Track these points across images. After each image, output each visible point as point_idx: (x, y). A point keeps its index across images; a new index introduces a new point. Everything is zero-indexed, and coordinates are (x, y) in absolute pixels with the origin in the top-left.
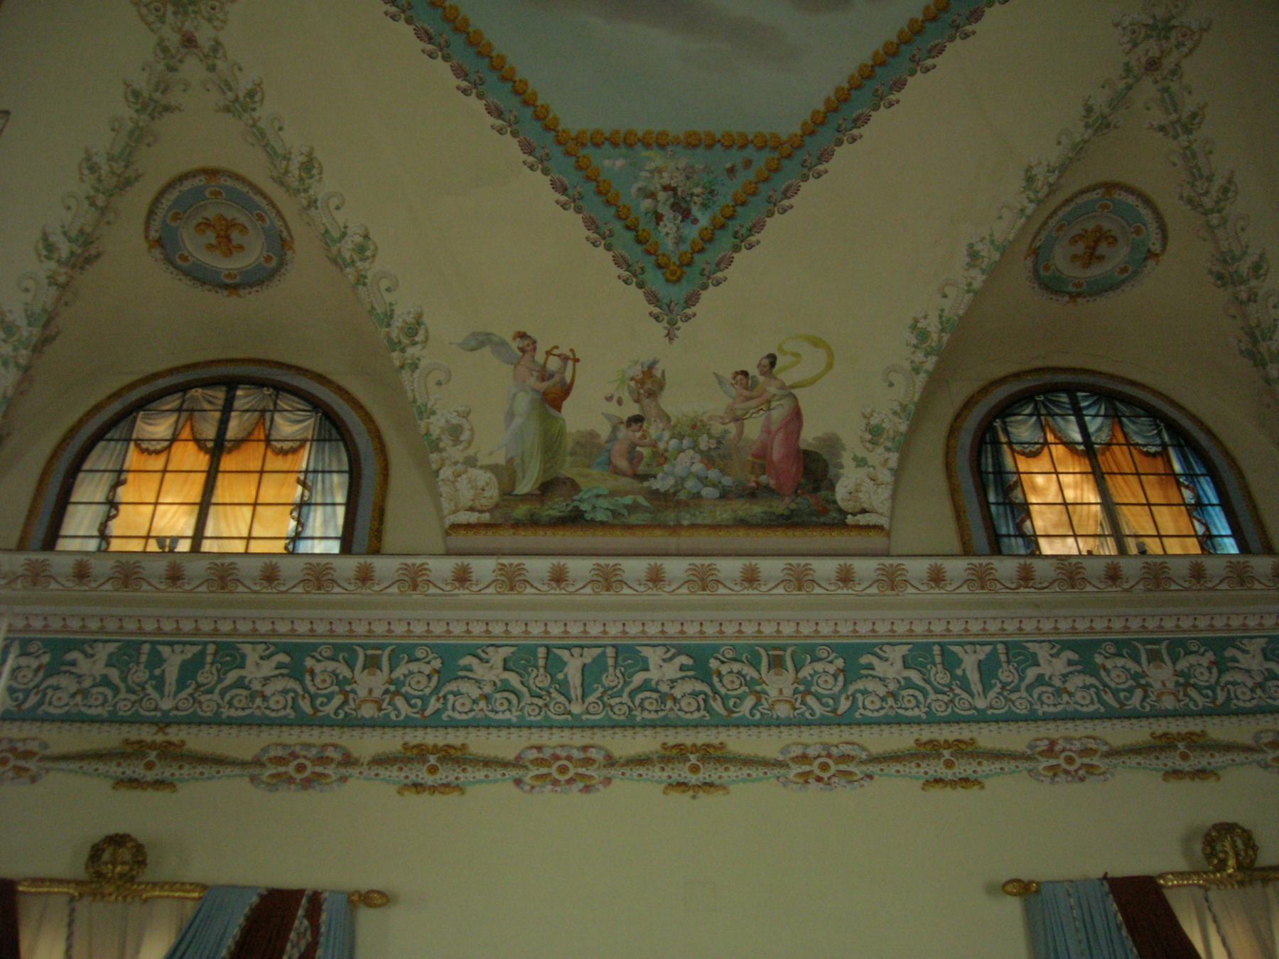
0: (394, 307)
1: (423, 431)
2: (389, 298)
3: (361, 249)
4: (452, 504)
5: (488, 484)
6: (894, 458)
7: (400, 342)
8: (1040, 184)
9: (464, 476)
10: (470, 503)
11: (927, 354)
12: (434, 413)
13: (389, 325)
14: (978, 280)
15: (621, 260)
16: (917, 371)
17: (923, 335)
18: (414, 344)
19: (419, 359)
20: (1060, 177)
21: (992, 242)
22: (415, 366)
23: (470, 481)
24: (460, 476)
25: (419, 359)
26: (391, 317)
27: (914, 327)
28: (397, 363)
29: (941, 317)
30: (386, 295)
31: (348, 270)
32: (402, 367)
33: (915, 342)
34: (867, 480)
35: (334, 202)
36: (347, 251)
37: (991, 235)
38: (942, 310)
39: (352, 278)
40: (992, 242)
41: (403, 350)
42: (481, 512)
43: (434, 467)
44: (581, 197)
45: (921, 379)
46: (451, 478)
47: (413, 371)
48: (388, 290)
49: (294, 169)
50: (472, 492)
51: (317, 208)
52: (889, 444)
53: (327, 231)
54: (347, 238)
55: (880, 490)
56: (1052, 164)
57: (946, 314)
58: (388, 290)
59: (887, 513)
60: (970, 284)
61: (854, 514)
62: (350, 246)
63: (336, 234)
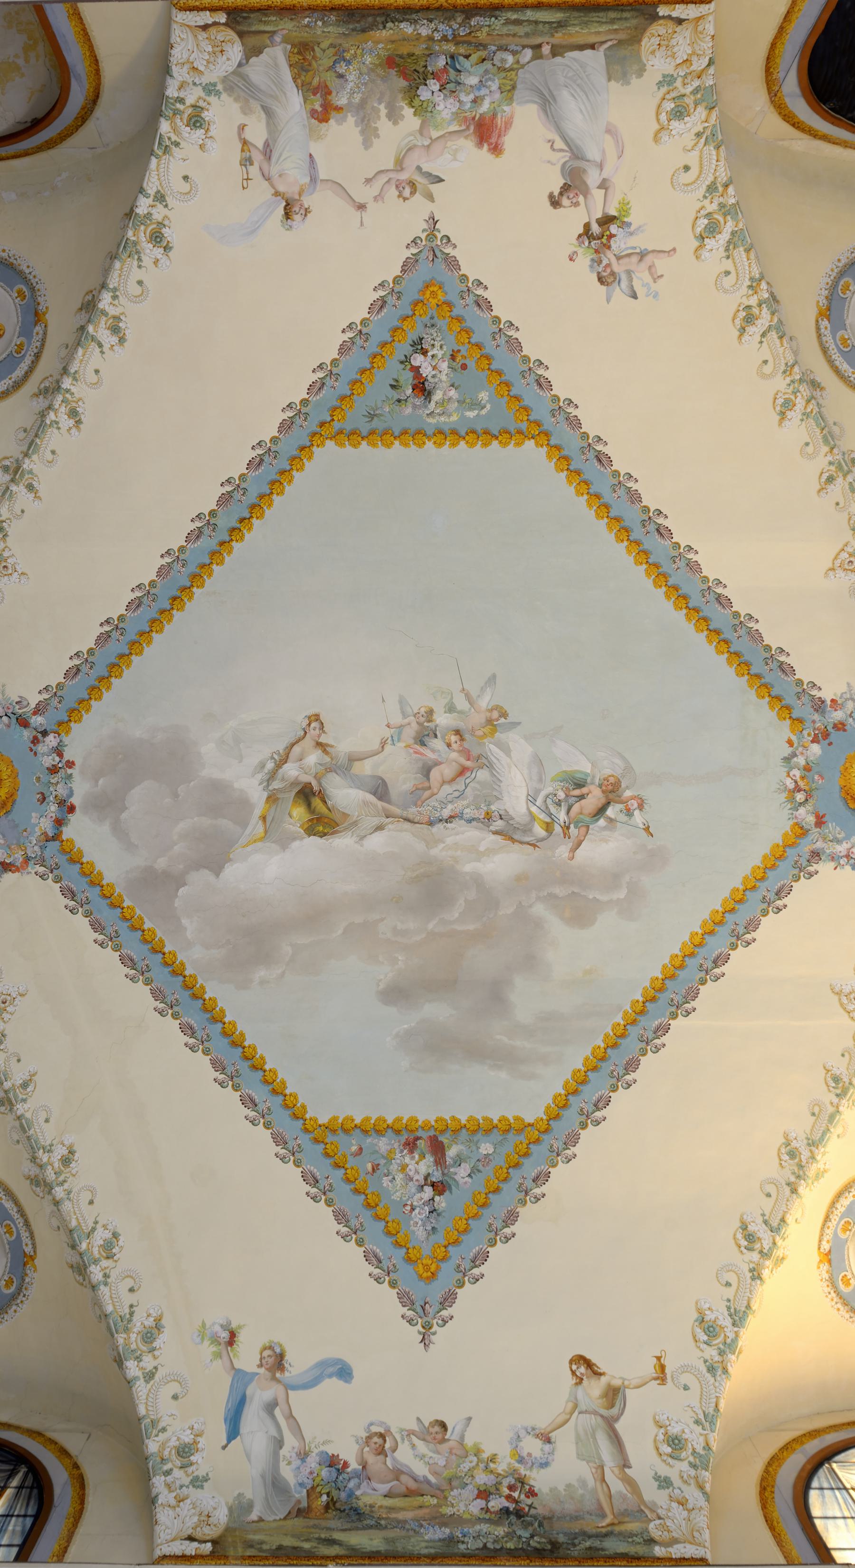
0: (724, 254)
1: (714, 114)
2: (728, 265)
3: (750, 319)
4: (700, 28)
5: (653, 52)
6: (172, 92)
7: (725, 215)
8: (63, 409)
9: (679, 61)
10: (679, 29)
11: (149, 215)
12: (698, 135)
13: (733, 233)
14: (105, 301)
15: (484, 306)
16: (160, 198)
17: (157, 238)
18: (709, 215)
19: (705, 197)
20: (43, 415)
21: (100, 345)
22: (712, 188)
23: (673, 56)
24: (684, 61)
25: (705, 197)
26: (729, 242)
27: (167, 248)
28: (731, 190)
29: (139, 259)
30: (731, 268)
31: (766, 295)
32: (726, 186)
33: (164, 230)
34: (202, 68)
35: (767, 369)
36: (765, 319)
37: (102, 352)
38: (140, 267)
39: (764, 285)
40: (100, 345)
41: (722, 206)
42: (669, 17)
43: (712, 70)
44: (523, 374)
45: (151, 185)
46: (694, 59)
47: (714, 183)
48: (727, 273)
49: (800, 402)
50: (673, 42)
51: (786, 364)
52: (179, 106)
53: (781, 338)
54: (761, 332)
55: (185, 56)
56: (55, 431)
57: (135, 263)
58: (727, 273)
59: (174, 26)
60: (115, 297)
61: (215, 24)
62: (758, 322)
63: (774, 335)
